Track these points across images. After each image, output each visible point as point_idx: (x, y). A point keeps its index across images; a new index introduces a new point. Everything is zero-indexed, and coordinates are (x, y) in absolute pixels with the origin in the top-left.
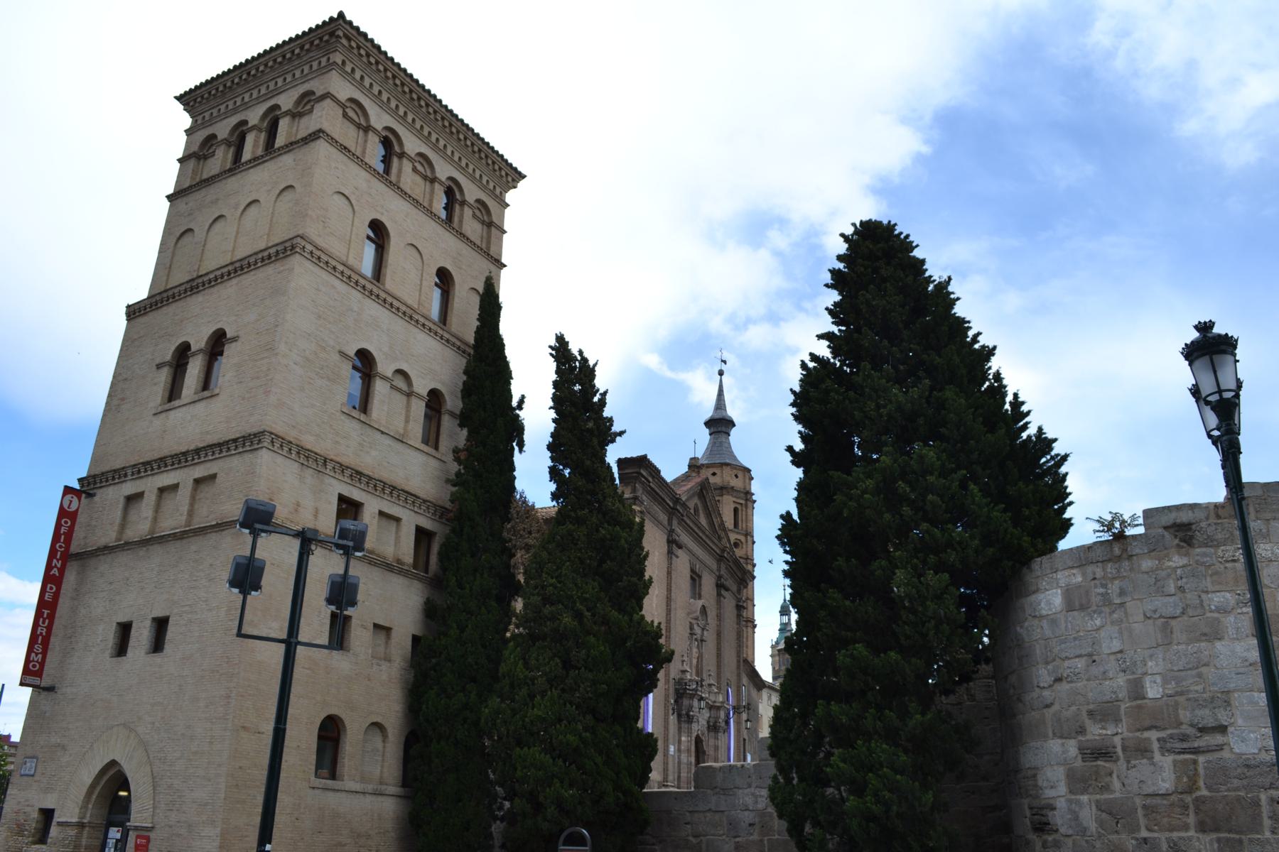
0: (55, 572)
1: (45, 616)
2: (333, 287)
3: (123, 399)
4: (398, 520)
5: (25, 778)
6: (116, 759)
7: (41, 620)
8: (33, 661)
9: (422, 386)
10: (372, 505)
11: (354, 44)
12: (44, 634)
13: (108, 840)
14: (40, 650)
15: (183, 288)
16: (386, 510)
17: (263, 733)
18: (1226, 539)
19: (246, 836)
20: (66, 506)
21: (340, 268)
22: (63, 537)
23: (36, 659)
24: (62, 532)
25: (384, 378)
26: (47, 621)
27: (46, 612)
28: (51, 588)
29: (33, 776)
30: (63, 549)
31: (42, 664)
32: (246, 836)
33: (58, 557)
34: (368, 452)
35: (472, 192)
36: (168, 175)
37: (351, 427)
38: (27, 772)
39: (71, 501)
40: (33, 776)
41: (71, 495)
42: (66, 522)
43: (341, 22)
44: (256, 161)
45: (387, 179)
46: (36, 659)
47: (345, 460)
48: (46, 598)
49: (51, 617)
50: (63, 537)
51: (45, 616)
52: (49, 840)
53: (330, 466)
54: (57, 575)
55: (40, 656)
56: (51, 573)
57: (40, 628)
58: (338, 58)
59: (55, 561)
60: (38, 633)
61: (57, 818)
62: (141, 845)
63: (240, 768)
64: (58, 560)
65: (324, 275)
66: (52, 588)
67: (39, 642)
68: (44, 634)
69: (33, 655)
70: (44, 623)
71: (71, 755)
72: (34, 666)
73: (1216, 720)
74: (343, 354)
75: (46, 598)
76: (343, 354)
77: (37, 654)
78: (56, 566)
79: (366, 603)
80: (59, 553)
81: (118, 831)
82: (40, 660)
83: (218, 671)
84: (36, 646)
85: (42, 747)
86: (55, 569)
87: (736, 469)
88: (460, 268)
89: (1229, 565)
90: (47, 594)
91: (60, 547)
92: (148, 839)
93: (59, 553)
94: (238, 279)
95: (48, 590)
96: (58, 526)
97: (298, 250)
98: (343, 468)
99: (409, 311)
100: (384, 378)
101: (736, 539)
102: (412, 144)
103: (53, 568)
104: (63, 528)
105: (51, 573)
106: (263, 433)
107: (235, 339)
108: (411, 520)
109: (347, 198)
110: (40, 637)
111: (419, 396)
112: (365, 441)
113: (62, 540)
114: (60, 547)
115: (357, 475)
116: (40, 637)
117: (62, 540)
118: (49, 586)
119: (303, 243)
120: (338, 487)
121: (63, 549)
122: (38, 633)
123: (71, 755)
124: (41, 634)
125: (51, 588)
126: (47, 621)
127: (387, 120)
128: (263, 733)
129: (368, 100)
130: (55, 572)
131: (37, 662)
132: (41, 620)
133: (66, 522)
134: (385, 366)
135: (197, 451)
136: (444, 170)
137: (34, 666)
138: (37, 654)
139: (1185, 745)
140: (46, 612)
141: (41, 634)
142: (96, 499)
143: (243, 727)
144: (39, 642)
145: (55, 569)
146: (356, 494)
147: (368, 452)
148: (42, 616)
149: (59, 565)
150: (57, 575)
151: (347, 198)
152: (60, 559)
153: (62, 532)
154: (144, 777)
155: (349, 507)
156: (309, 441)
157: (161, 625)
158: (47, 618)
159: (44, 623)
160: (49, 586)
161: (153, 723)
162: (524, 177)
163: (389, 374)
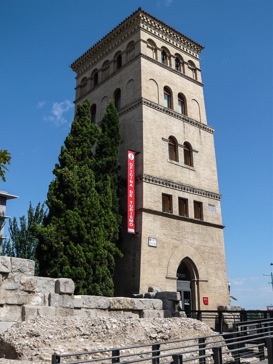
1: (131, 204)
7: (130, 205)
8: (130, 222)
12: (132, 211)
14: (132, 218)
22: (131, 170)
23: (131, 222)
24: (131, 169)
26: (132, 205)
28: (131, 192)
30: (132, 176)
33: (131, 179)
39: (131, 156)
41: (131, 153)
46: (131, 222)
48: (130, 196)
50: (131, 170)
51: (131, 204)
54: (132, 186)
55: (132, 220)
56: (130, 186)
59: (130, 181)
60: (130, 211)
67: (131, 214)
68: (132, 211)
70: (131, 207)
72: (131, 224)
78: (131, 183)
82: (133, 222)
84: (130, 216)
90: (130, 194)
93: (131, 177)
95: (130, 193)
104: (131, 167)
105: (130, 186)
110: (131, 212)
116: (131, 212)
118: (130, 191)
121: (132, 176)
122: (130, 211)
124: (131, 211)
125: (131, 192)
126: (132, 205)
131: (132, 223)
132: (130, 205)
137: (131, 224)
141: (131, 211)
144: (131, 214)
145: (131, 184)
149: (132, 183)
150: (132, 186)
152: (132, 180)
153: (131, 169)
160: (130, 191)
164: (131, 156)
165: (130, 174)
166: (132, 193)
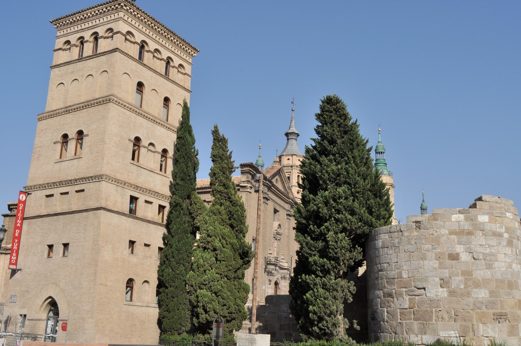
0: (19, 225)
1: (16, 242)
2: (125, 113)
3: (40, 155)
5: (12, 303)
6: (51, 296)
7: (15, 244)
8: (13, 259)
13: (48, 325)
14: (15, 255)
15: (63, 110)
16: (147, 200)
17: (107, 286)
18: (430, 227)
19: (104, 322)
20: (21, 199)
22: (21, 211)
25: (144, 147)
26: (17, 244)
27: (16, 240)
28: (18, 231)
29: (15, 302)
31: (16, 260)
32: (104, 322)
34: (140, 177)
38: (12, 301)
39: (23, 197)
40: (15, 302)
42: (21, 205)
44: (90, 57)
45: (142, 63)
47: (132, 182)
48: (16, 235)
49: (19, 242)
50: (21, 211)
51: (16, 242)
52: (25, 326)
53: (127, 185)
55: (15, 257)
56: (17, 225)
57: (14, 247)
59: (18, 221)
61: (27, 317)
62: (64, 326)
63: (101, 298)
64: (19, 220)
65: (122, 110)
66: (18, 231)
67: (15, 252)
69: (13, 257)
70: (16, 245)
71: (31, 294)
72: (13, 261)
73: (423, 286)
74: (130, 140)
75: (16, 235)
76: (130, 140)
77: (14, 257)
78: (19, 223)
79: (141, 236)
80: (20, 217)
81: (52, 322)
83: (90, 264)
84: (13, 254)
85: (18, 292)
86: (19, 224)
87: (299, 157)
88: (173, 96)
89: (431, 236)
91: (20, 215)
92: (66, 324)
93: (20, 217)
94: (86, 110)
95: (17, 232)
97: (111, 101)
98: (131, 185)
99: (154, 118)
100: (144, 147)
101: (298, 190)
103: (18, 223)
105: (17, 225)
106: (103, 175)
107: (87, 135)
109: (128, 75)
110: (15, 250)
111: (158, 153)
112: (139, 173)
113: (20, 212)
114: (20, 215)
115: (137, 187)
116: (15, 250)
117: (20, 212)
118: (17, 230)
119: (113, 98)
123: (31, 294)
125: (18, 231)
126: (17, 244)
128: (107, 286)
132: (15, 244)
133: (21, 205)
134: (145, 142)
135: (76, 180)
136: (165, 54)
137: (13, 261)
138: (14, 257)
139: (412, 293)
140: (16, 240)
142: (32, 195)
143: (101, 284)
144: (15, 252)
145: (19, 224)
146: (136, 195)
148: (15, 242)
149: (20, 222)
151: (128, 75)
154: (63, 302)
155: (133, 199)
156: (119, 176)
157: (66, 245)
158: (17, 243)
159: (16, 245)
160: (17, 230)
161: (66, 283)
163: (147, 145)
164: (23, 197)
165: (19, 214)
166: (19, 232)
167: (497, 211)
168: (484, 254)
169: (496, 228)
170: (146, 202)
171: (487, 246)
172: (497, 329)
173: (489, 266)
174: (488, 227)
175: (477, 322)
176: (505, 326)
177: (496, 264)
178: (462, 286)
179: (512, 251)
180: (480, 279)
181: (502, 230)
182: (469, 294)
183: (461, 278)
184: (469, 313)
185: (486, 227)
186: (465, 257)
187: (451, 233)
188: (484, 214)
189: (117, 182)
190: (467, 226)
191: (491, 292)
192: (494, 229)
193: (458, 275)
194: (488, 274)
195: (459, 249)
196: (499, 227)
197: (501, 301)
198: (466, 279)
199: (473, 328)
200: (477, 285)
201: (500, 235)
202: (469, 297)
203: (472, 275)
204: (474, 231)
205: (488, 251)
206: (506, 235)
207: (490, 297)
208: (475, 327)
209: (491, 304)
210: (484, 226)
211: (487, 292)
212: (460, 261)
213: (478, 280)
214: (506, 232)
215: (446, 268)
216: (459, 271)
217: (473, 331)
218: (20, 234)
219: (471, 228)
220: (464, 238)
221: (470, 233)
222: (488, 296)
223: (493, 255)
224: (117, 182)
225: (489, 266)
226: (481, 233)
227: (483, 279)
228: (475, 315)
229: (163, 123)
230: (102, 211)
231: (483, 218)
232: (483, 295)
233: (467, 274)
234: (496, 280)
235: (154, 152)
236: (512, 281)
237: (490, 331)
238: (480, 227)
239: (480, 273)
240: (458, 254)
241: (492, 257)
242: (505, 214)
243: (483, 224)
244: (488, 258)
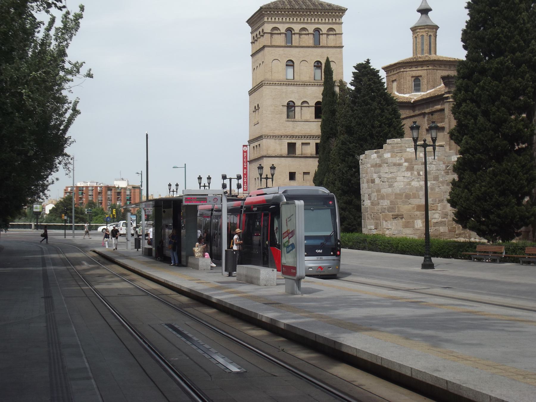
4: (309, 143)
9: (312, 103)
10: (299, 143)
11: (268, 12)
21: (277, 83)
27: (245, 176)
35: (324, 28)
36: (249, 49)
37: (290, 124)
43: (262, 9)
53: (283, 137)
58: (266, 19)
66: (245, 170)
96: (244, 155)
102: (297, 28)
108: (313, 143)
115: (292, 137)
119: (264, 82)
120: (286, 141)
127: (287, 26)
129: (278, 24)
130: (245, 166)
134: (298, 103)
140: (245, 176)
147: (296, 128)
156: (277, 133)
162: (347, 9)
163: (300, 104)
167: (398, 149)
168: (387, 178)
169: (396, 160)
170: (303, 144)
171: (389, 173)
172: (394, 224)
173: (391, 186)
174: (390, 161)
175: (383, 220)
176: (400, 222)
177: (395, 184)
178: (376, 199)
179: (412, 174)
180: (385, 194)
181: (401, 161)
182: (379, 204)
183: (375, 194)
184: (378, 215)
185: (389, 161)
186: (377, 181)
187: (372, 166)
188: (388, 152)
189: (275, 137)
190: (378, 161)
191: (391, 202)
192: (394, 161)
193: (374, 193)
194: (390, 190)
195: (375, 176)
196: (398, 159)
197: (398, 207)
198: (377, 194)
199: (380, 224)
200: (383, 198)
201: (400, 165)
202: (379, 205)
203: (380, 192)
204: (382, 165)
205: (390, 176)
206: (406, 164)
207: (391, 205)
208: (382, 223)
209: (391, 209)
210: (388, 160)
211: (389, 202)
212: (375, 184)
213: (384, 195)
214: (406, 161)
215: (370, 189)
216: (375, 190)
217: (381, 226)
218: (247, 172)
219: (380, 163)
220: (377, 169)
221: (380, 166)
222: (389, 204)
223: (393, 178)
224: (275, 137)
225: (391, 186)
226: (386, 165)
227: (386, 194)
228: (381, 216)
229: (312, 83)
230: (265, 159)
231: (387, 155)
232: (386, 204)
233: (379, 191)
234: (395, 194)
235: (309, 107)
236: (410, 194)
237: (389, 225)
238: (385, 162)
239: (385, 190)
240: (374, 179)
241: (393, 180)
242: (406, 150)
243: (387, 159)
244: (390, 181)
